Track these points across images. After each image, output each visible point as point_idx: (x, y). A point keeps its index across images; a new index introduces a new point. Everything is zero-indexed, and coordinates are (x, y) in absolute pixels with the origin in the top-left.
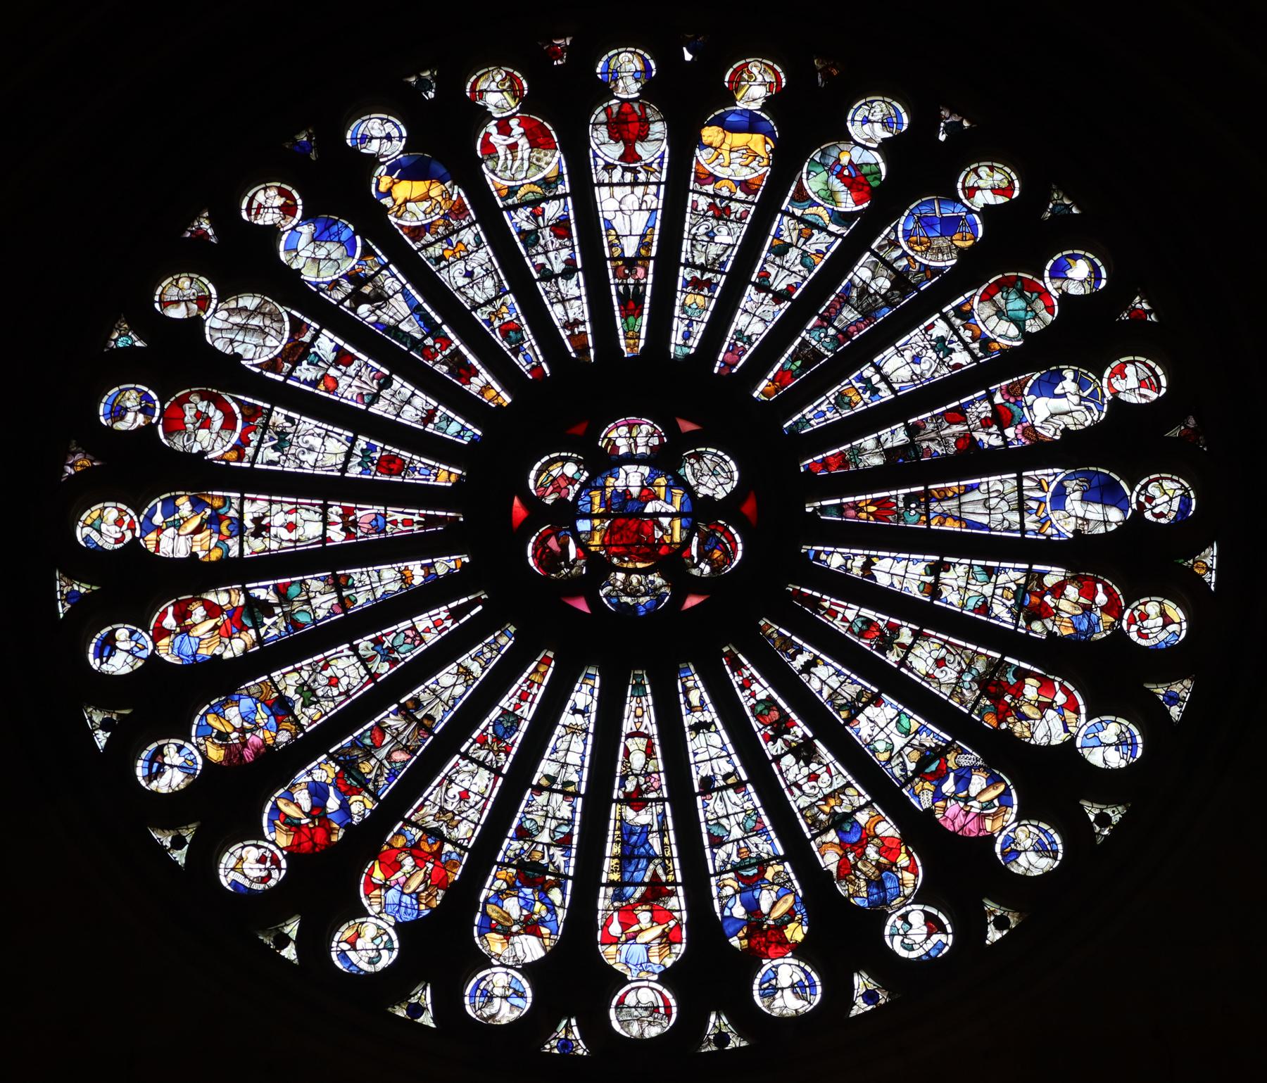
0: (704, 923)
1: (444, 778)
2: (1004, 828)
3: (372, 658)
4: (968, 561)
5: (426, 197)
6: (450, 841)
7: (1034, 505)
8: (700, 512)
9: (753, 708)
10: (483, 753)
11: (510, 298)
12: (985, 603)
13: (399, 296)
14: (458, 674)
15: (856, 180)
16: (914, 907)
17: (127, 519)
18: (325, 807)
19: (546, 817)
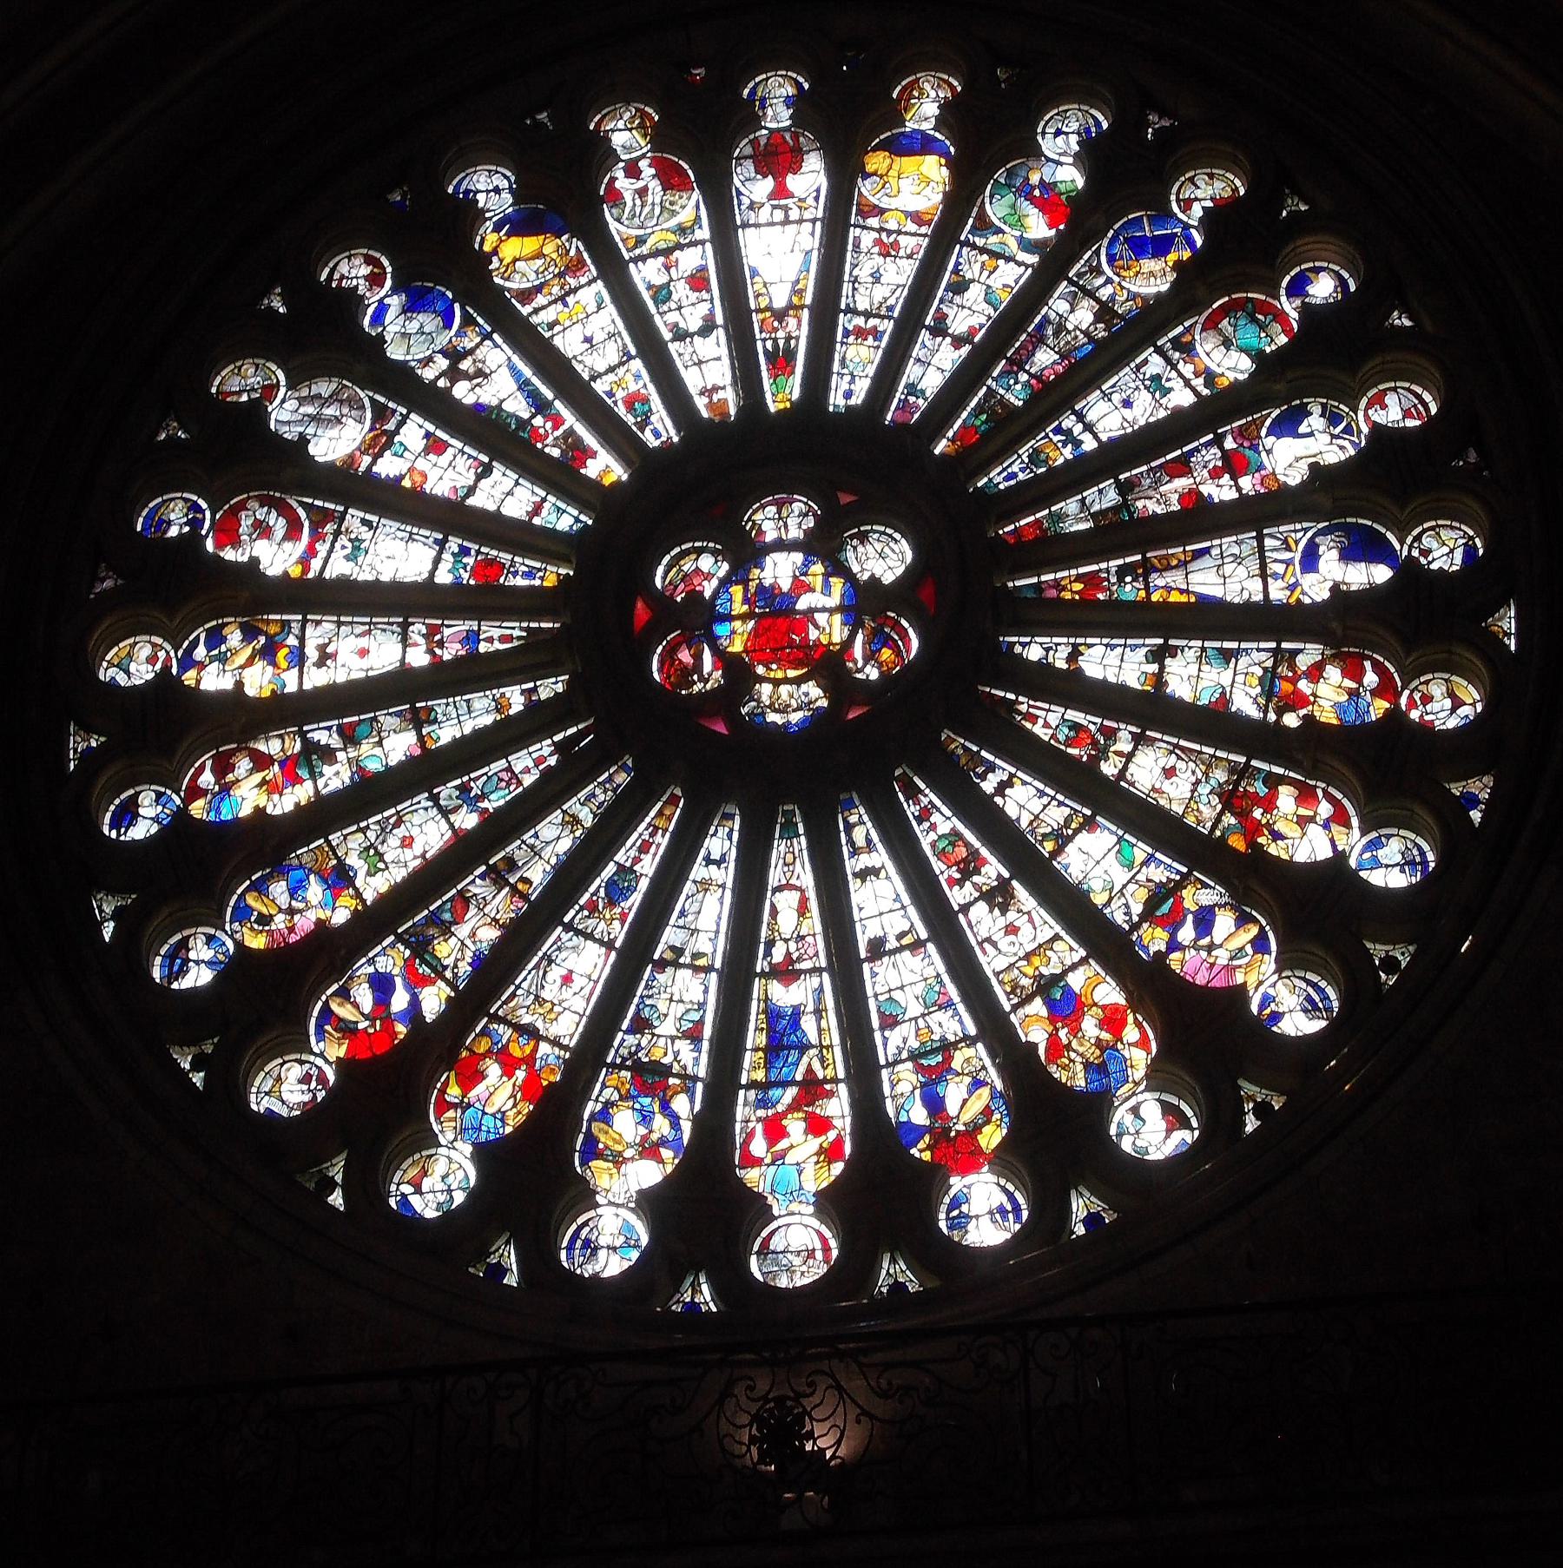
1: (542, 959)
2: (1261, 983)
3: (456, 810)
4: (1199, 643)
5: (540, 255)
6: (546, 1039)
7: (1280, 568)
8: (866, 601)
9: (933, 845)
11: (637, 365)
12: (1223, 694)
13: (505, 371)
14: (564, 824)
15: (1048, 199)
16: (1147, 1095)
17: (162, 655)
18: (389, 1004)
19: (671, 1000)
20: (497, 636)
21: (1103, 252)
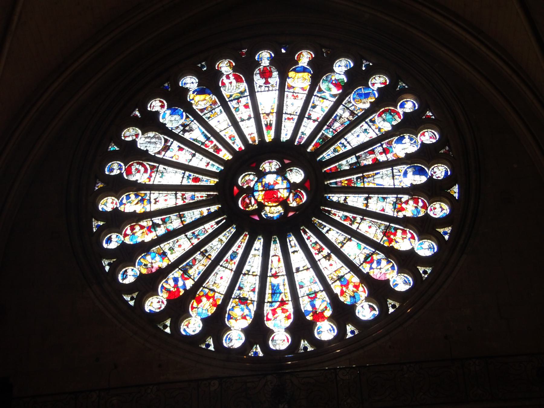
0: (298, 313)
3: (192, 238)
5: (205, 100)
8: (293, 187)
10: (227, 264)
13: (198, 129)
14: (219, 241)
15: (337, 84)
17: (115, 202)
20: (200, 196)
21: (352, 97)
